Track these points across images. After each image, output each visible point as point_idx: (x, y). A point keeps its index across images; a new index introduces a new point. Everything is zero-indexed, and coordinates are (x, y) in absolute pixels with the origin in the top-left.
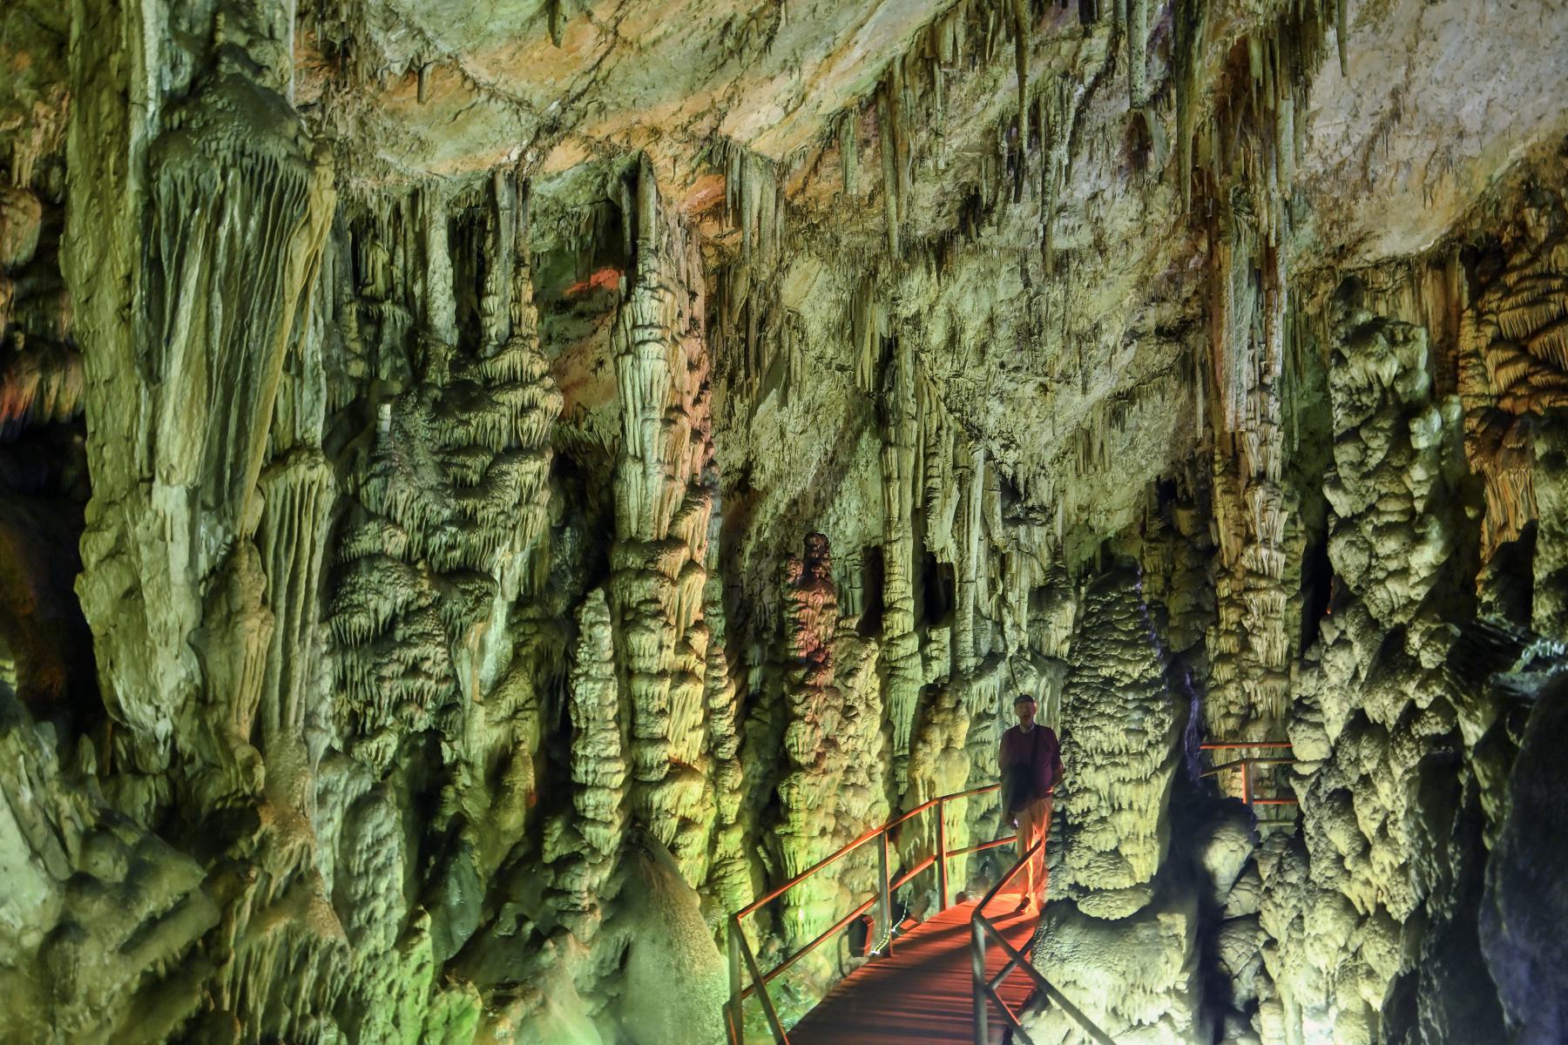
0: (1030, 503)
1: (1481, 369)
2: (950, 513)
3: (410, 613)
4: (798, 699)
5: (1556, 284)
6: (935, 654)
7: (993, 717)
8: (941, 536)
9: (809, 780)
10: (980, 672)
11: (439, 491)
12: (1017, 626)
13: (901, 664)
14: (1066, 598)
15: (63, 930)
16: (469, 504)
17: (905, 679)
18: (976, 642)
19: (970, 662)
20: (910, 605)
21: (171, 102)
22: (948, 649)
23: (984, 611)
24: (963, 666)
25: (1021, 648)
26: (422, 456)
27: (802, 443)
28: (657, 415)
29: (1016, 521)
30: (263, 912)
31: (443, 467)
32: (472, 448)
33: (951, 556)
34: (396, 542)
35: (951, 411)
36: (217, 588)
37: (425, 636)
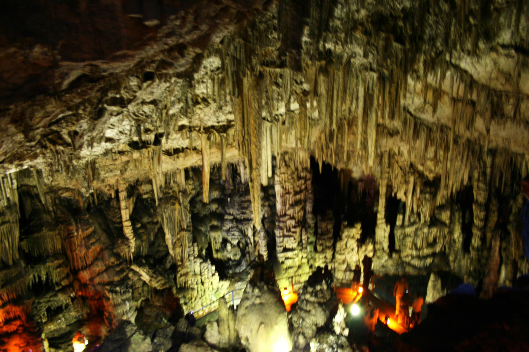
3: (232, 228)
8: (401, 195)
11: (238, 210)
12: (425, 217)
14: (447, 208)
15: (151, 280)
16: (244, 211)
19: (406, 223)
21: (160, 199)
26: (236, 204)
28: (279, 196)
30: (181, 276)
31: (240, 205)
32: (245, 202)
33: (404, 199)
34: (232, 217)
35: (401, 168)
36: (174, 245)
37: (235, 231)
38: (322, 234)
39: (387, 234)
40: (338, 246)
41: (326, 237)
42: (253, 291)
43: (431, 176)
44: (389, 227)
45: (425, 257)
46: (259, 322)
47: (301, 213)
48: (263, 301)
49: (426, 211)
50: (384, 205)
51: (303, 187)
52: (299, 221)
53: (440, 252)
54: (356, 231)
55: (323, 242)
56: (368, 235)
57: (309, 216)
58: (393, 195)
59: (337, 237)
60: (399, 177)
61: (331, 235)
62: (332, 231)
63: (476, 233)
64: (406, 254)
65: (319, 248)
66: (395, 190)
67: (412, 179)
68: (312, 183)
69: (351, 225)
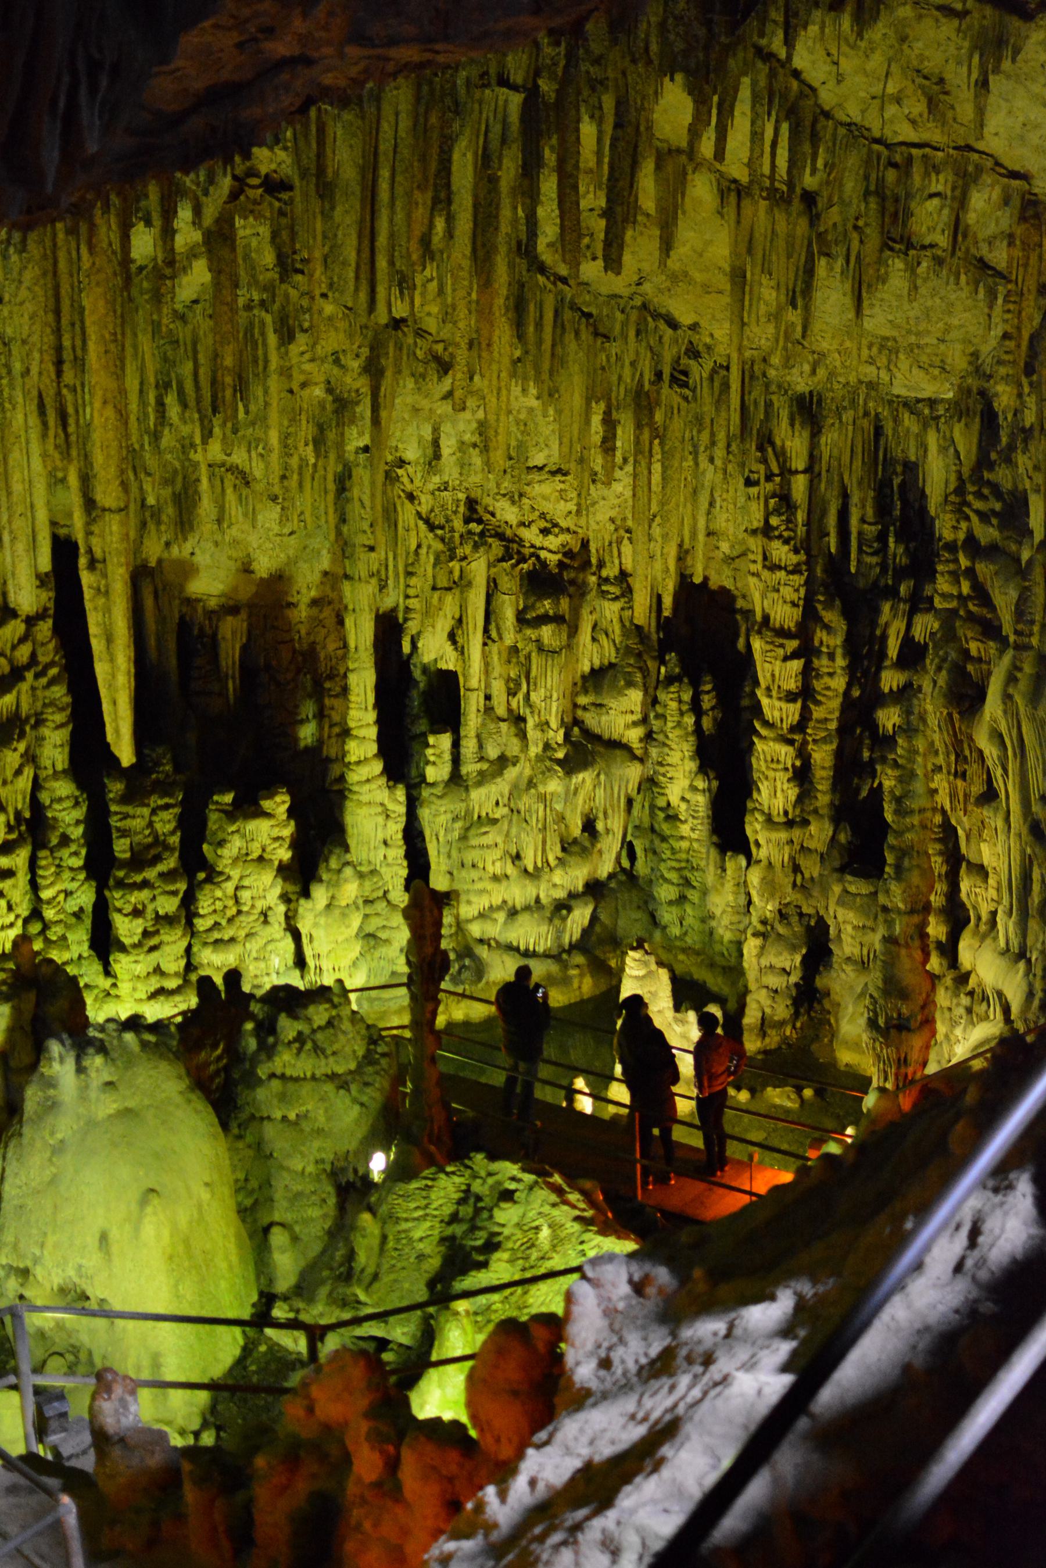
0: (604, 573)
1: (952, 567)
2: (443, 625)
4: (117, 894)
5: (998, 506)
6: (432, 758)
7: (495, 821)
8: (433, 649)
9: (132, 958)
10: (483, 778)
12: (544, 726)
13: (355, 788)
14: (630, 684)
17: (359, 803)
18: (481, 747)
19: (470, 768)
20: (372, 732)
22: (447, 756)
23: (501, 711)
24: (464, 770)
25: (547, 746)
27: (292, 541)
29: (544, 619)
33: (450, 662)
35: (432, 527)
38: (140, 860)
39: (395, 829)
40: (204, 904)
41: (151, 874)
42: (80, 1070)
43: (551, 549)
44: (401, 793)
45: (562, 907)
46: (134, 1194)
47: (24, 783)
48: (131, 1104)
49: (548, 698)
50: (371, 699)
51: (23, 653)
52: (18, 814)
53: (611, 876)
54: (271, 831)
55: (144, 895)
56: (316, 847)
57: (64, 788)
58: (406, 648)
59: (196, 868)
60: (427, 561)
61: (171, 862)
62: (175, 840)
63: (771, 759)
64: (481, 903)
65: (127, 929)
66: (412, 627)
67: (479, 568)
68: (56, 630)
69: (248, 807)
